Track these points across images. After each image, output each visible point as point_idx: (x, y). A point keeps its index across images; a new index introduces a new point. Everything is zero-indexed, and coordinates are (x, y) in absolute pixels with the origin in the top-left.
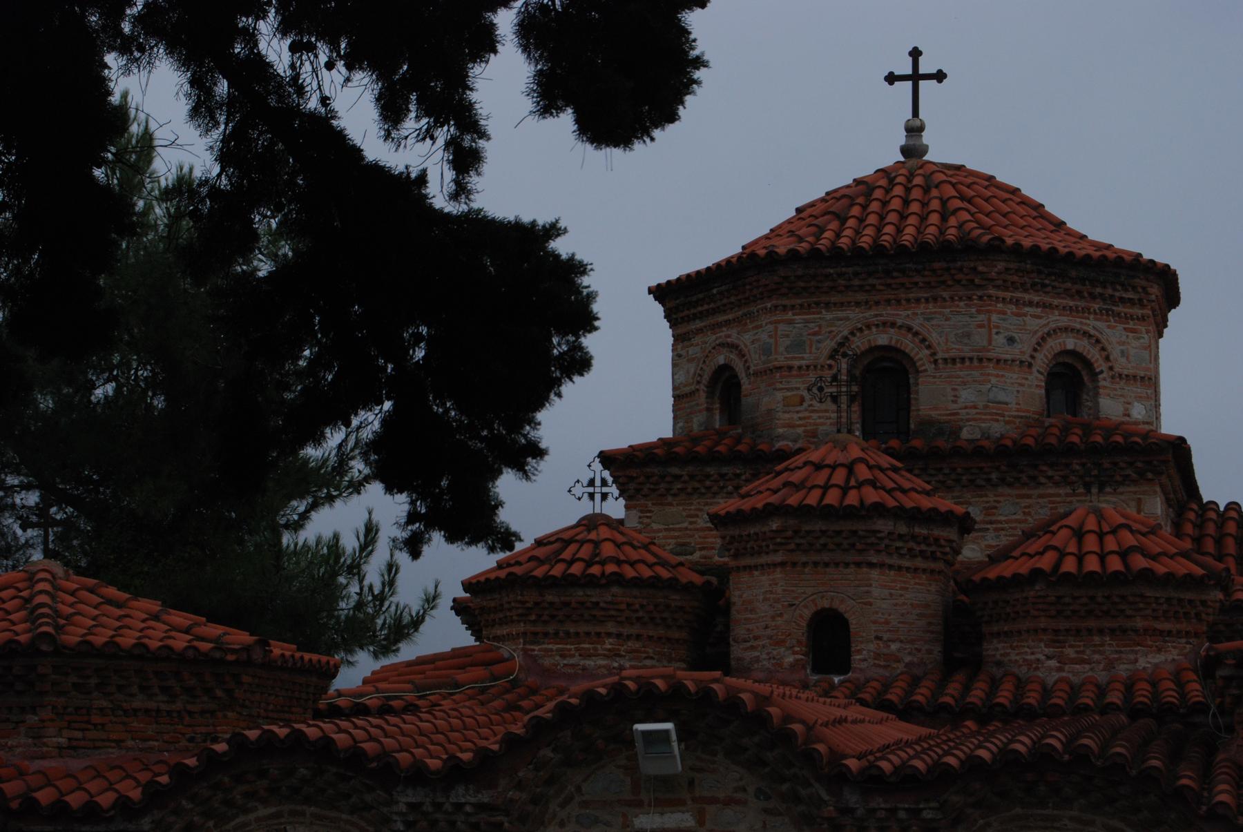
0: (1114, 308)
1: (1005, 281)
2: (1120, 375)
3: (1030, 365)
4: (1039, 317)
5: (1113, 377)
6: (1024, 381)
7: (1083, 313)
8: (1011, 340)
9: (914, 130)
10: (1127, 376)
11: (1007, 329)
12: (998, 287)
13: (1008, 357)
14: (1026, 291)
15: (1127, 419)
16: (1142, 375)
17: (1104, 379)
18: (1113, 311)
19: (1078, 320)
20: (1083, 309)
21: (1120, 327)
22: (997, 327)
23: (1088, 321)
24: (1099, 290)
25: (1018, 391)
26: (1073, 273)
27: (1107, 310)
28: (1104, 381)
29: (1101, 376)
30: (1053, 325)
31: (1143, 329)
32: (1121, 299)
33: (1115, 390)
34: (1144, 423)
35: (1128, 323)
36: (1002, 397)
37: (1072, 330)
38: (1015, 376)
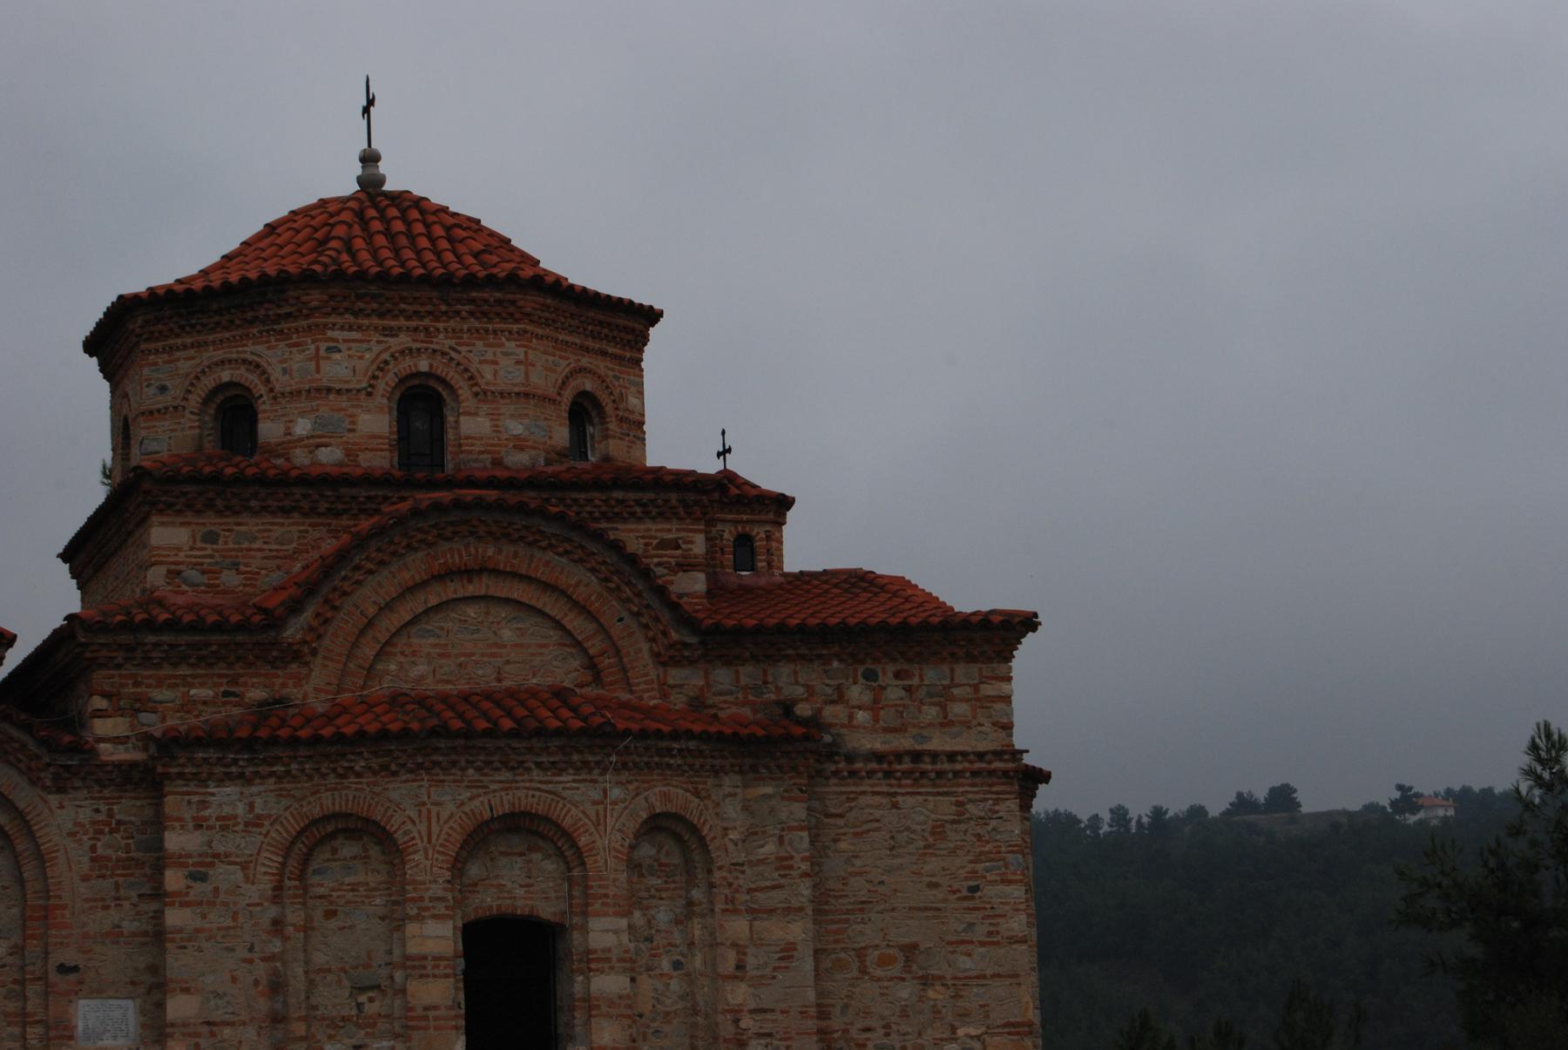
0: (275, 327)
1: (152, 333)
2: (283, 394)
3: (184, 408)
4: (193, 358)
5: (275, 398)
6: (176, 426)
7: (241, 341)
8: (163, 389)
9: (370, 158)
10: (291, 393)
11: (158, 379)
12: (146, 340)
13: (160, 406)
14: (178, 336)
15: (289, 437)
16: (307, 388)
17: (264, 403)
18: (274, 330)
19: (234, 350)
20: (241, 337)
21: (282, 344)
22: (146, 380)
23: (246, 348)
24: (250, 315)
25: (170, 438)
26: (215, 306)
27: (268, 331)
28: (264, 406)
29: (260, 401)
30: (206, 363)
31: (310, 341)
32: (279, 315)
33: (277, 411)
34: (308, 438)
35: (291, 338)
36: (154, 447)
37: (230, 361)
38: (166, 423)
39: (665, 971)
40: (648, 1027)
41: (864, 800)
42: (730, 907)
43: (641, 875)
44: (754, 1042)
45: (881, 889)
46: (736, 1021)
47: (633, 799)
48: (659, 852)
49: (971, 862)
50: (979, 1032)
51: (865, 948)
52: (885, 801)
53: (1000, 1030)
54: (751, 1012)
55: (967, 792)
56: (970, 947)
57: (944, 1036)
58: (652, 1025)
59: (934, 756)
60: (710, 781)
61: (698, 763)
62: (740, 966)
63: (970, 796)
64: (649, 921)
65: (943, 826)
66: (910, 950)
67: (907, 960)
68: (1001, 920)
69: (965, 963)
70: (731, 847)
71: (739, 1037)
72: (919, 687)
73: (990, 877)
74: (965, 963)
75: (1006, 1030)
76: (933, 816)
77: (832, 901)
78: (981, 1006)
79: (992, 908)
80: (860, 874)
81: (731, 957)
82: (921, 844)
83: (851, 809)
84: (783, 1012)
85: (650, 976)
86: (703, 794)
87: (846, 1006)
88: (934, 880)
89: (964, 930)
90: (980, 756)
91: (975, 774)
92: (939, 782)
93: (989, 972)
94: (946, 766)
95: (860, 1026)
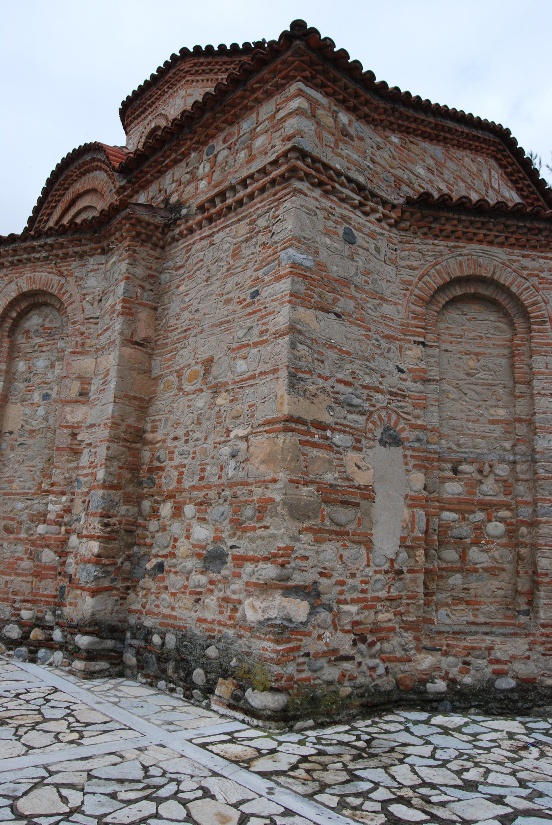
39: (36, 401)
40: (16, 440)
41: (197, 246)
42: (80, 349)
43: (29, 338)
44: (86, 451)
45: (198, 316)
46: (74, 435)
47: (6, 285)
48: (44, 320)
49: (256, 270)
50: (245, 432)
51: (182, 369)
52: (205, 243)
53: (261, 429)
54: (87, 427)
55: (258, 209)
56: (248, 349)
57: (222, 439)
58: (19, 439)
59: (232, 188)
60: (77, 263)
61: (60, 253)
62: (83, 393)
63: (259, 212)
64: (29, 368)
65: (240, 247)
66: (209, 363)
67: (207, 372)
68: (271, 317)
69: (241, 366)
70: (87, 306)
71: (74, 447)
72: (237, 140)
73: (267, 279)
74: (241, 366)
75: (266, 428)
76: (234, 241)
77: (169, 335)
78: (250, 406)
79: (265, 308)
80: (186, 308)
81: (75, 387)
82: (225, 268)
83: (189, 257)
84: (99, 425)
85: (22, 405)
86: (65, 273)
87: (167, 420)
88: (229, 296)
89: (245, 335)
90: (263, 171)
91: (262, 190)
92: (239, 210)
93: (257, 372)
94: (241, 194)
95: (172, 436)
